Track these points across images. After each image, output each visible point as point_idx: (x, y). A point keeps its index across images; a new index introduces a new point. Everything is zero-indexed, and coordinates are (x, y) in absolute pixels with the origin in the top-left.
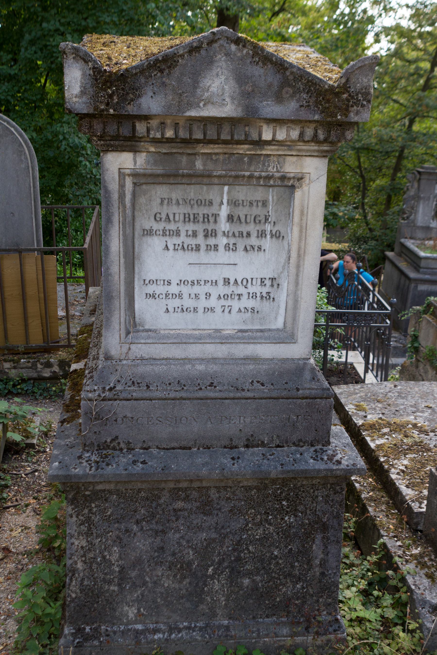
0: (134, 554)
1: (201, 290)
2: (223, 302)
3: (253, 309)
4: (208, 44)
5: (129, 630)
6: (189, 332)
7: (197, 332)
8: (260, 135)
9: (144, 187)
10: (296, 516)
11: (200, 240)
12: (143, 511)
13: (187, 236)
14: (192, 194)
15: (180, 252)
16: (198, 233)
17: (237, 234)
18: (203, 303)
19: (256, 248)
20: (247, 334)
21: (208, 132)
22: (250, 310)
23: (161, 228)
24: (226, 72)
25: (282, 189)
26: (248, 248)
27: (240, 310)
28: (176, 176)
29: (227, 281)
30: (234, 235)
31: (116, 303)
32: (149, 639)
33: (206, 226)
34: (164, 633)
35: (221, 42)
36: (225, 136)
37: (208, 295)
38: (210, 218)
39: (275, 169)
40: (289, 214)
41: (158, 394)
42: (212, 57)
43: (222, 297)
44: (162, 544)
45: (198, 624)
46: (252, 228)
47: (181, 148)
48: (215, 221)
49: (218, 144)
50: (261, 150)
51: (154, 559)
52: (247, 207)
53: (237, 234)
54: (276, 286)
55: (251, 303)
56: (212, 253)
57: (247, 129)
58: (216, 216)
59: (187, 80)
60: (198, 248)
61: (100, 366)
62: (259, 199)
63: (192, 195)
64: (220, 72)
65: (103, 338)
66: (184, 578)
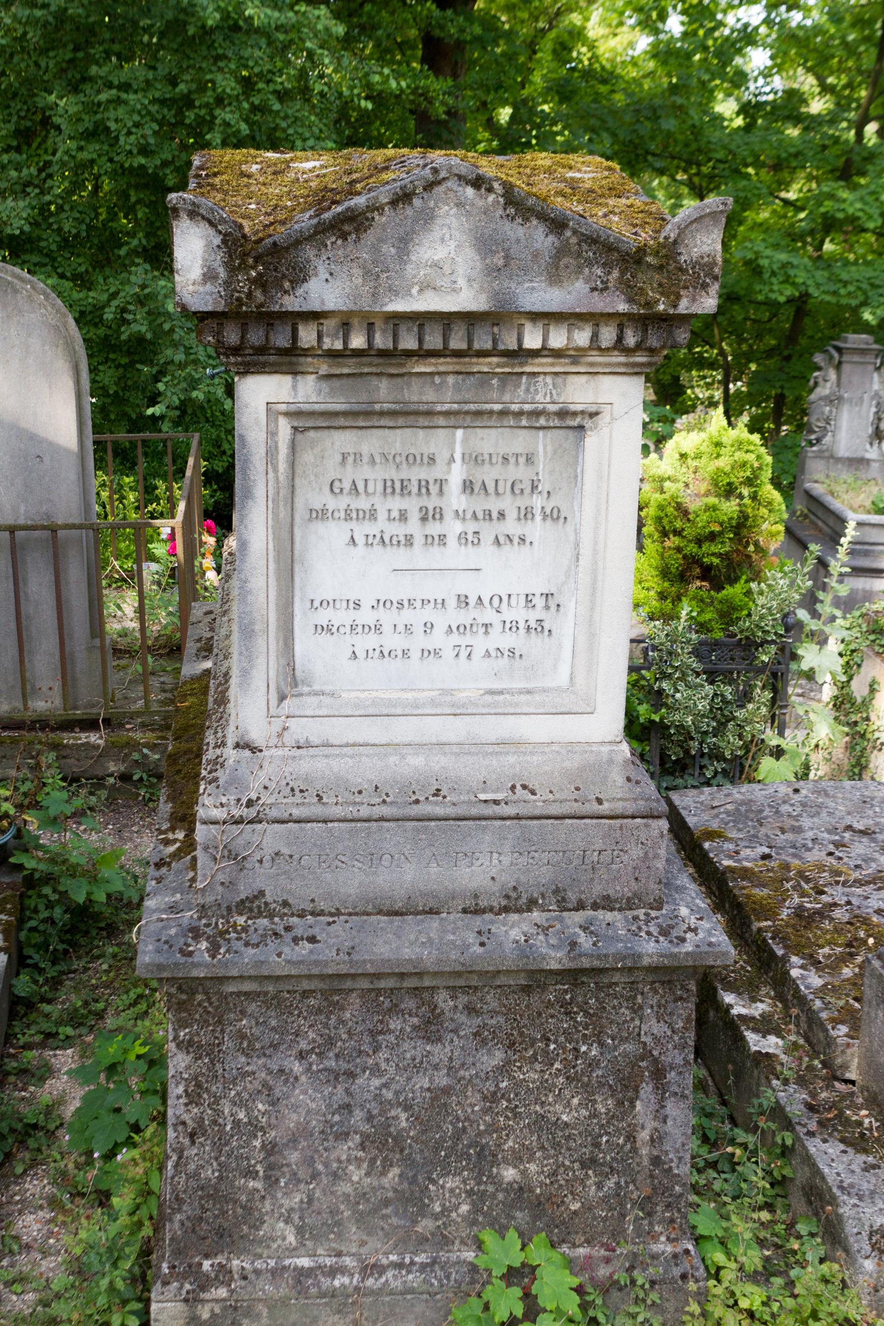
0: (294, 1117)
1: (416, 617)
2: (455, 639)
3: (512, 651)
4: (425, 189)
5: (285, 1268)
6: (395, 696)
7: (409, 695)
8: (520, 341)
9: (312, 434)
10: (601, 1044)
11: (414, 526)
12: (311, 1035)
13: (389, 519)
14: (398, 445)
15: (378, 549)
16: (409, 515)
17: (480, 515)
18: (419, 642)
19: (516, 540)
20: (502, 697)
21: (427, 338)
22: (506, 653)
23: (343, 506)
24: (457, 234)
25: (562, 432)
26: (502, 539)
27: (488, 654)
28: (368, 414)
29: (463, 601)
30: (475, 516)
31: (261, 642)
32: (324, 1287)
33: (425, 501)
34: (352, 1275)
35: (449, 184)
36: (457, 342)
37: (429, 627)
38: (431, 487)
39: (548, 399)
40: (576, 477)
41: (338, 811)
42: (433, 209)
43: (454, 629)
44: (347, 1100)
45: (417, 1259)
46: (508, 503)
47: (376, 365)
48: (441, 492)
49: (445, 356)
50: (522, 364)
51: (332, 1127)
52: (499, 466)
53: (480, 515)
54: (553, 608)
55: (507, 641)
56: (436, 550)
57: (496, 330)
58: (441, 483)
59: (389, 250)
60: (409, 541)
61: (231, 761)
62: (519, 451)
63: (398, 447)
64: (447, 236)
65: (231, 705)
66: (387, 1165)
